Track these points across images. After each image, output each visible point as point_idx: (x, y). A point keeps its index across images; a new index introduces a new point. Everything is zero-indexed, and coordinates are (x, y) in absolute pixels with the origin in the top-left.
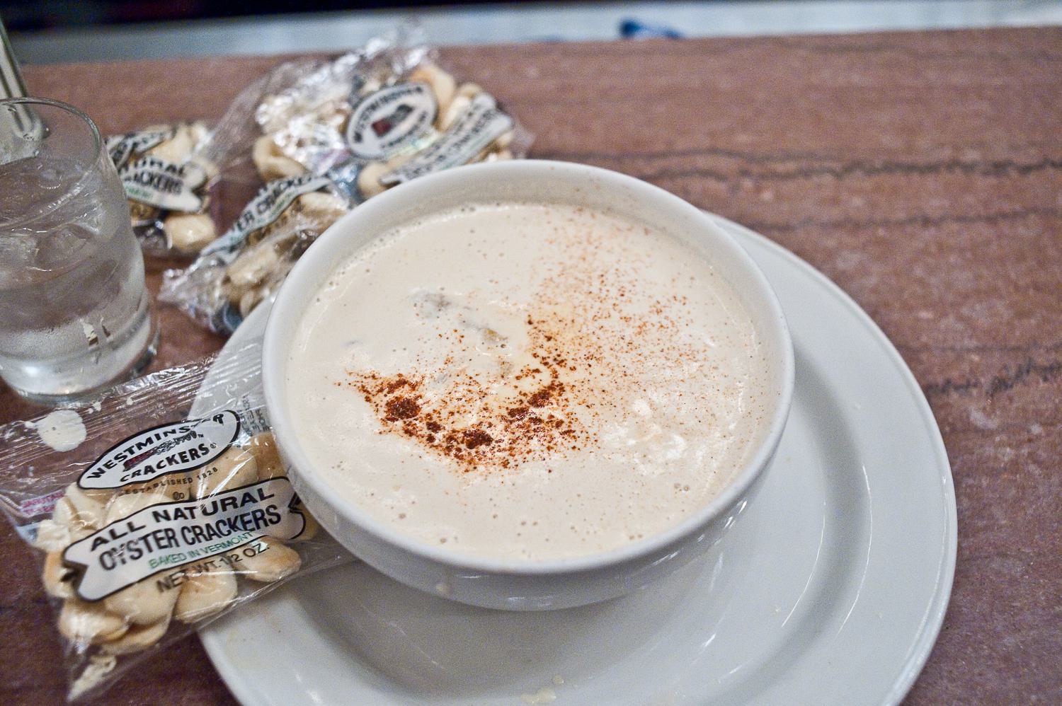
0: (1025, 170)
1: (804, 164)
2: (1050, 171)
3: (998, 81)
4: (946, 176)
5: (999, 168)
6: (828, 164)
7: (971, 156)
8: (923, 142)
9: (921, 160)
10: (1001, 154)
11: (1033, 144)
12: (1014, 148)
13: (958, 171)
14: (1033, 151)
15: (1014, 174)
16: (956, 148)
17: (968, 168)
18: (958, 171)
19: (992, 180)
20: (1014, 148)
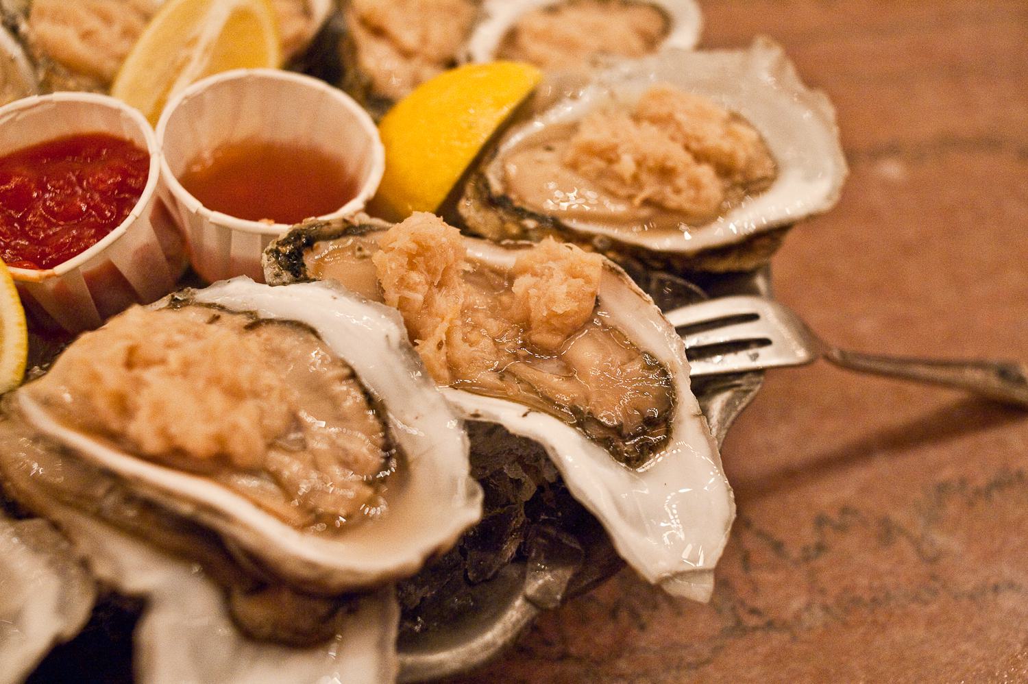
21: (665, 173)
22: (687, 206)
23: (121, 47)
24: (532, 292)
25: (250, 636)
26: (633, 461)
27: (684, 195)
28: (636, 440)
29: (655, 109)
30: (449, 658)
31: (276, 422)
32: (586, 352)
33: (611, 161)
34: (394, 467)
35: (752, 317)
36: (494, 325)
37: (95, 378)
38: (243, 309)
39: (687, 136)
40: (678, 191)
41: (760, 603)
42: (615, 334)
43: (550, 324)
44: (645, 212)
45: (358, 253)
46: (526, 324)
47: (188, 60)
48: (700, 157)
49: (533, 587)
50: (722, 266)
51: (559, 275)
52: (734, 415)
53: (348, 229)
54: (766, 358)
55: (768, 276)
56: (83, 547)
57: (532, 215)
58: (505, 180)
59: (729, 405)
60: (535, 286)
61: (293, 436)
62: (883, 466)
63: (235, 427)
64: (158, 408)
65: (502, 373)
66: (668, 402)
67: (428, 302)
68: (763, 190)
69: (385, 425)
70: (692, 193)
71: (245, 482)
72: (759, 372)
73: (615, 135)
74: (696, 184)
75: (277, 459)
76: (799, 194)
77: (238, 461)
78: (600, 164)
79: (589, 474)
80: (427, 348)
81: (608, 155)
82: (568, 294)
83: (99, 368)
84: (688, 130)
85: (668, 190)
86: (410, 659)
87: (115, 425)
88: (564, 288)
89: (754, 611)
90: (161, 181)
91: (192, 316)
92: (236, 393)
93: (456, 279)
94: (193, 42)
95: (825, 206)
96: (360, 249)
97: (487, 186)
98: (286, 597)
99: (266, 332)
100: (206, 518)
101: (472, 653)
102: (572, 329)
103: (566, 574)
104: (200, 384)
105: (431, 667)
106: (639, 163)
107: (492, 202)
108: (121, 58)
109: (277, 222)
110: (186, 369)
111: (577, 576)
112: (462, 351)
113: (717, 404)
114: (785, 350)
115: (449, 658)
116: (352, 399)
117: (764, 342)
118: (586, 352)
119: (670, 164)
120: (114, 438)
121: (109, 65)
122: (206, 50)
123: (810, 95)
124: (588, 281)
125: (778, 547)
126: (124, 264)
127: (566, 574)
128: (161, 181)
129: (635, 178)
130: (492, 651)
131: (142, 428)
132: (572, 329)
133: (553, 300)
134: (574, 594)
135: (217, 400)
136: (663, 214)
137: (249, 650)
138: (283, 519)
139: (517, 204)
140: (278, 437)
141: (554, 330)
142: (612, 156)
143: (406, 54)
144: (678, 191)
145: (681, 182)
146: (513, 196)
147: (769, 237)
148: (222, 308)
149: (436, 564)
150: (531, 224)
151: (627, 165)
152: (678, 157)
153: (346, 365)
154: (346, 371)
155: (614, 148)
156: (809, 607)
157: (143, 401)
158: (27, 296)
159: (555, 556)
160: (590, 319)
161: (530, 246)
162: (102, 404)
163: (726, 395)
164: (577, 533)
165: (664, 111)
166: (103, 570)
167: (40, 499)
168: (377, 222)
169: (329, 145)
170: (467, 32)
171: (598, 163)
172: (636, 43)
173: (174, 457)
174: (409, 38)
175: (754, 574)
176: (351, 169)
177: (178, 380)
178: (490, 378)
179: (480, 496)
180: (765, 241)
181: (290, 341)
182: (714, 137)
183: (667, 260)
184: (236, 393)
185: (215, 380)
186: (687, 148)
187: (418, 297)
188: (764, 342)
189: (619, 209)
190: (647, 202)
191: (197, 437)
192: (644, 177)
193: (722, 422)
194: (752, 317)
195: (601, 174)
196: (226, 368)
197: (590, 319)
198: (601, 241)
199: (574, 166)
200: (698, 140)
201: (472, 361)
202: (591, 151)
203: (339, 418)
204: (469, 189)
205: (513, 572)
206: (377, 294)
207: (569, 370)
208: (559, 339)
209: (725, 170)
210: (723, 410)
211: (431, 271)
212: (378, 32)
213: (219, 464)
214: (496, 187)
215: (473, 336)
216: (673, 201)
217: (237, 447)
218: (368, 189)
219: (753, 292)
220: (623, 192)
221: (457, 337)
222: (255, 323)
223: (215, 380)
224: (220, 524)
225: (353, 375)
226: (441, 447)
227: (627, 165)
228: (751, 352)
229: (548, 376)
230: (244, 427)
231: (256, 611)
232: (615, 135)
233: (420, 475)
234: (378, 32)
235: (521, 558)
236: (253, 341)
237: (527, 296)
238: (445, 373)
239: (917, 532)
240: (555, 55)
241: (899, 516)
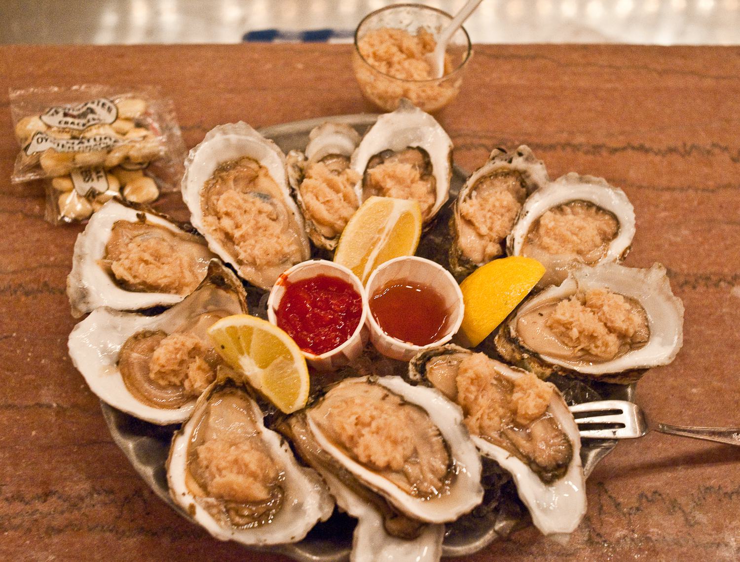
0: (614, 151)
1: (469, 141)
2: (630, 152)
3: (609, 86)
4: (560, 153)
5: (597, 149)
6: (484, 141)
7: (580, 139)
8: (550, 129)
9: (546, 141)
10: (600, 138)
11: (622, 133)
12: (610, 135)
13: (569, 149)
14: (621, 138)
15: (605, 153)
16: (572, 133)
17: (576, 148)
18: (569, 149)
19: (590, 157)
20: (610, 135)
21: (592, 337)
22: (599, 354)
23: (346, 212)
24: (520, 401)
25: (389, 534)
26: (548, 482)
27: (599, 349)
28: (550, 473)
29: (594, 301)
30: (461, 550)
31: (408, 452)
32: (538, 429)
33: (568, 329)
34: (450, 475)
35: (619, 412)
36: (501, 411)
37: (343, 428)
38: (399, 393)
39: (606, 318)
40: (597, 347)
41: (602, 532)
42: (552, 421)
43: (525, 416)
44: (580, 354)
45: (449, 364)
46: (515, 412)
47: (379, 239)
48: (611, 330)
49: (499, 525)
50: (612, 381)
51: (533, 396)
52: (599, 459)
53: (445, 352)
54: (621, 433)
55: (634, 388)
56: (333, 491)
57: (527, 351)
58: (517, 331)
59: (598, 455)
60: (521, 398)
61: (413, 459)
62: (682, 472)
63: (394, 458)
64: (367, 447)
65: (502, 434)
66: (570, 457)
67: (476, 398)
68: (639, 348)
69: (450, 456)
70: (603, 349)
71: (394, 476)
72: (616, 440)
73: (572, 317)
74: (606, 345)
75: (409, 468)
76: (655, 353)
77: (393, 469)
78: (563, 329)
79: (528, 486)
80: (473, 421)
81: (567, 326)
82: (535, 406)
83: (346, 426)
84: (608, 316)
85: (593, 345)
86: (447, 548)
87: (348, 445)
88: (534, 403)
89: (599, 535)
90: (367, 319)
91: (377, 392)
92: (395, 443)
93: (490, 387)
94: (381, 231)
95: (667, 362)
96: (450, 362)
97: (509, 332)
98: (405, 520)
99: (407, 409)
100: (381, 493)
101: (470, 549)
102: (533, 419)
103: (512, 523)
104: (383, 438)
105: (454, 552)
106: (580, 333)
107: (512, 341)
108: (346, 221)
109: (415, 344)
110: (377, 432)
111: (517, 524)
112: (486, 422)
113: (592, 454)
114: (630, 429)
115: (461, 550)
116: (438, 446)
117: (622, 426)
118: (538, 429)
119: (595, 335)
120: (346, 447)
121: (340, 223)
122: (387, 235)
123: (675, 298)
124: (545, 400)
125: (617, 505)
126: (347, 353)
127: (512, 523)
128: (367, 319)
129: (578, 339)
130: (478, 549)
131: (360, 451)
132: (533, 419)
133: (527, 407)
134: (514, 530)
135: (389, 446)
136: (587, 356)
137: (390, 539)
138: (408, 493)
139: (521, 343)
140: (409, 458)
141: (526, 418)
142: (569, 326)
143: (481, 236)
144: (597, 347)
145: (599, 343)
146: (520, 339)
147: (637, 373)
148: (389, 390)
149: (463, 518)
150: (526, 356)
151: (575, 333)
152: (601, 330)
153: (438, 430)
154: (438, 433)
155: (571, 323)
156: (625, 537)
157: (362, 441)
158: (308, 362)
159: (510, 515)
160: (543, 415)
161: (523, 372)
162: (344, 438)
163: (598, 450)
164: (521, 512)
165: (600, 303)
166: (341, 503)
167: (314, 463)
168: (458, 348)
169: (439, 290)
170: (514, 223)
171: (562, 330)
172: (598, 239)
173: (370, 466)
174: (484, 230)
175: (603, 516)
176: (448, 304)
177: (375, 435)
178: (495, 435)
179: (483, 493)
180: (635, 374)
181: (415, 415)
182: (620, 323)
183: (586, 378)
184: (395, 443)
185: (389, 437)
186: (605, 324)
187: (472, 397)
188: (622, 426)
189: (566, 351)
190: (582, 349)
191: (381, 461)
192: (582, 339)
193: (592, 463)
194: (619, 412)
195: (562, 334)
196: (393, 433)
197: (543, 415)
198: (556, 367)
199: (551, 327)
200: (612, 322)
201: (489, 427)
202: (559, 322)
203: (433, 452)
204: (500, 332)
205: (491, 517)
206: (453, 398)
207: (530, 437)
208: (528, 422)
209: (622, 336)
210: (595, 457)
211: (479, 386)
212: (469, 223)
213: (386, 470)
214: (513, 333)
215: (492, 415)
216: (594, 351)
217: (394, 465)
218: (454, 329)
219: (623, 397)
220: (570, 344)
221: (485, 417)
222: (404, 403)
223: (389, 437)
224: (386, 496)
225: (440, 434)
226: (470, 469)
227: (575, 333)
228: (614, 430)
229: (519, 437)
230: (397, 456)
231: (393, 525)
232: (572, 317)
233: (461, 481)
234: (469, 223)
235: (496, 510)
236: (403, 413)
237: (517, 402)
238: (478, 431)
239: (688, 510)
240: (555, 245)
241: (682, 500)
